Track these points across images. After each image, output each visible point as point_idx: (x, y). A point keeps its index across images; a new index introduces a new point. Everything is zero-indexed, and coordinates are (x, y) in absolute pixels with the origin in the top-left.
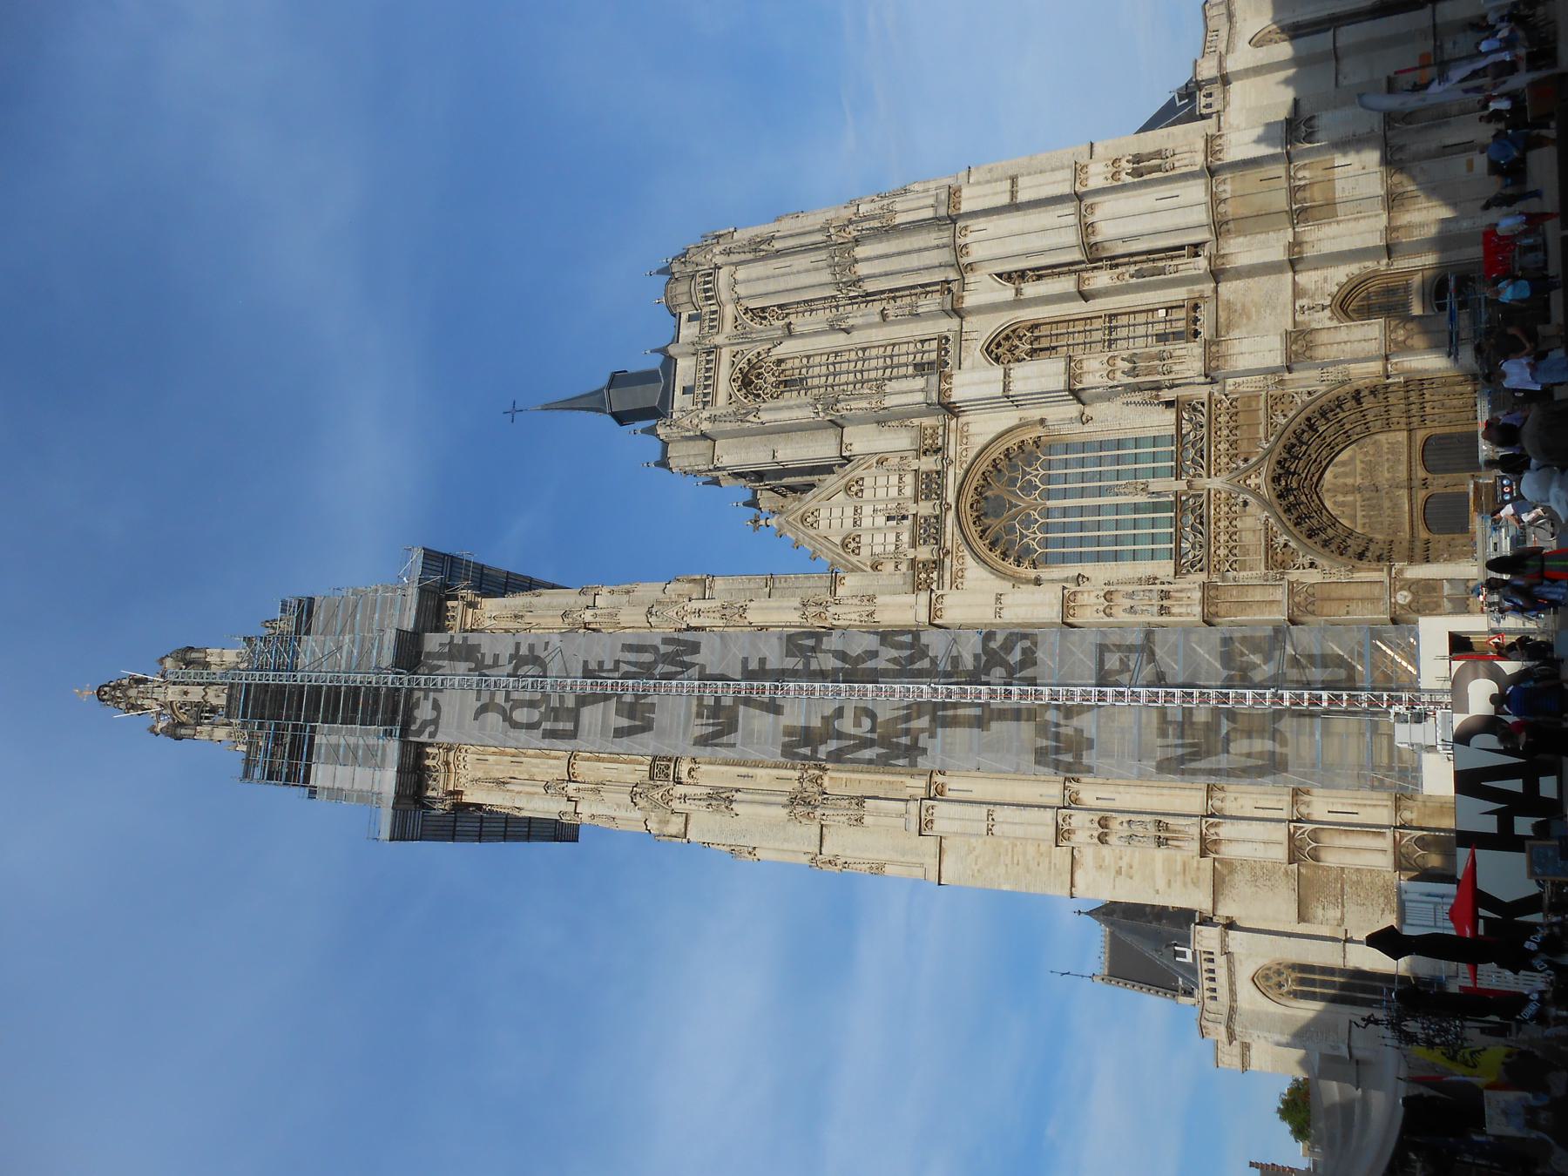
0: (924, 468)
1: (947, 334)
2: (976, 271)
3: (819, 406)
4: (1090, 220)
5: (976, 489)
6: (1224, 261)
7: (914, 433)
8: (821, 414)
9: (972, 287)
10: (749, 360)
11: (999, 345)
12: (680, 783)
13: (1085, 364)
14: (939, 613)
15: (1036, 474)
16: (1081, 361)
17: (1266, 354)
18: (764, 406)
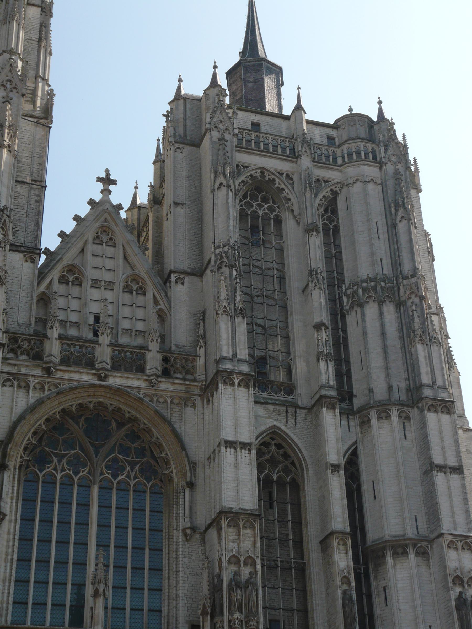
0: (149, 356)
1: (296, 392)
3: (226, 249)
5: (120, 409)
8: (217, 251)
9: (344, 422)
10: (283, 189)
11: (279, 446)
13: (249, 532)
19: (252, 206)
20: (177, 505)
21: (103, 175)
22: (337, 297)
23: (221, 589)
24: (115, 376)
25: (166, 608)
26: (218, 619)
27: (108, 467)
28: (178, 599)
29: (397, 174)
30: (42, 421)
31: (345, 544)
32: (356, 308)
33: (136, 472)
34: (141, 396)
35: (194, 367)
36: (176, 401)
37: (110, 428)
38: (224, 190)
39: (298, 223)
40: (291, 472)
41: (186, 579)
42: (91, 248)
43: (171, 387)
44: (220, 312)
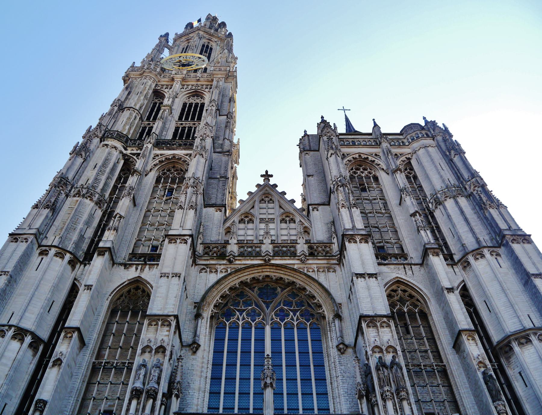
1: (409, 258)
2: (464, 270)
4: (533, 338)
5: (281, 278)
7: (326, 241)
8: (334, 183)
10: (374, 161)
11: (404, 291)
13: (387, 330)
15: (294, 319)
16: (389, 326)
18: (339, 159)
19: (357, 173)
20: (330, 332)
21: (265, 173)
22: (425, 207)
23: (370, 373)
24: (276, 259)
25: (333, 405)
26: (371, 396)
27: (276, 315)
28: (340, 397)
29: (445, 140)
30: (226, 289)
31: (474, 339)
32: (439, 207)
33: (298, 316)
35: (331, 250)
36: (321, 270)
37: (277, 292)
38: (333, 156)
39: (388, 174)
40: (418, 306)
41: (345, 381)
44: (340, 207)
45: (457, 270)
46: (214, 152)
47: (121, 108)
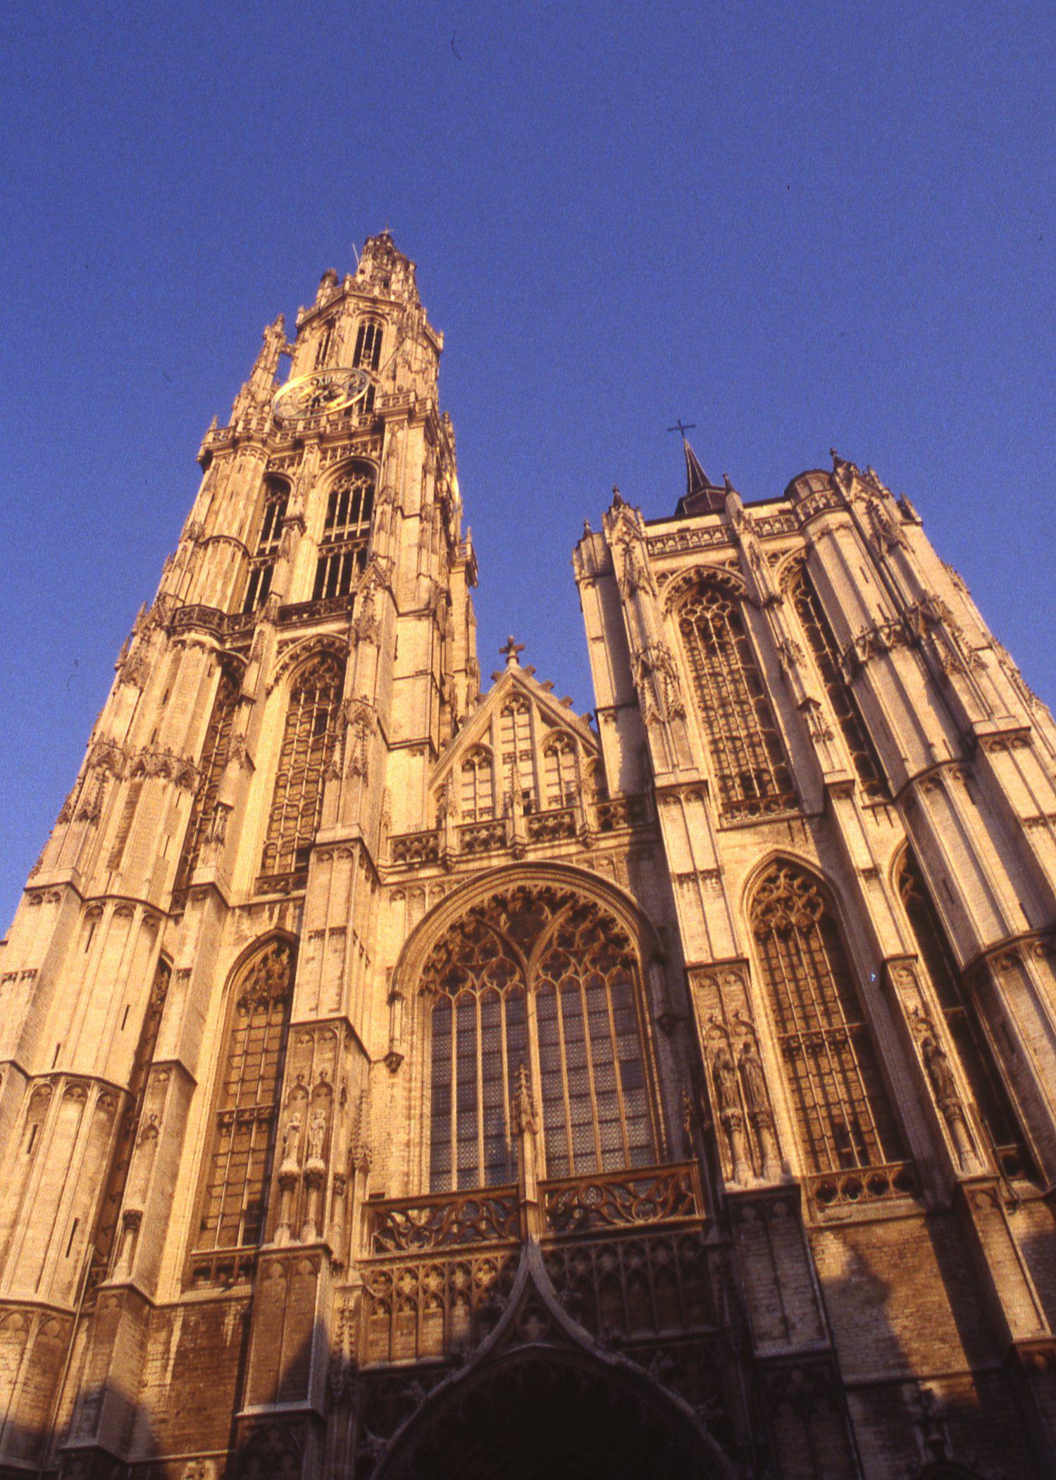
0: (577, 813)
5: (548, 889)
6: (988, 1209)
9: (882, 817)
12: (169, 636)
14: (326, 856)
17: (778, 1314)
27: (546, 968)
34: (574, 865)
42: (499, 722)
43: (612, 843)
45: (894, 815)
46: (400, 615)
47: (201, 540)
